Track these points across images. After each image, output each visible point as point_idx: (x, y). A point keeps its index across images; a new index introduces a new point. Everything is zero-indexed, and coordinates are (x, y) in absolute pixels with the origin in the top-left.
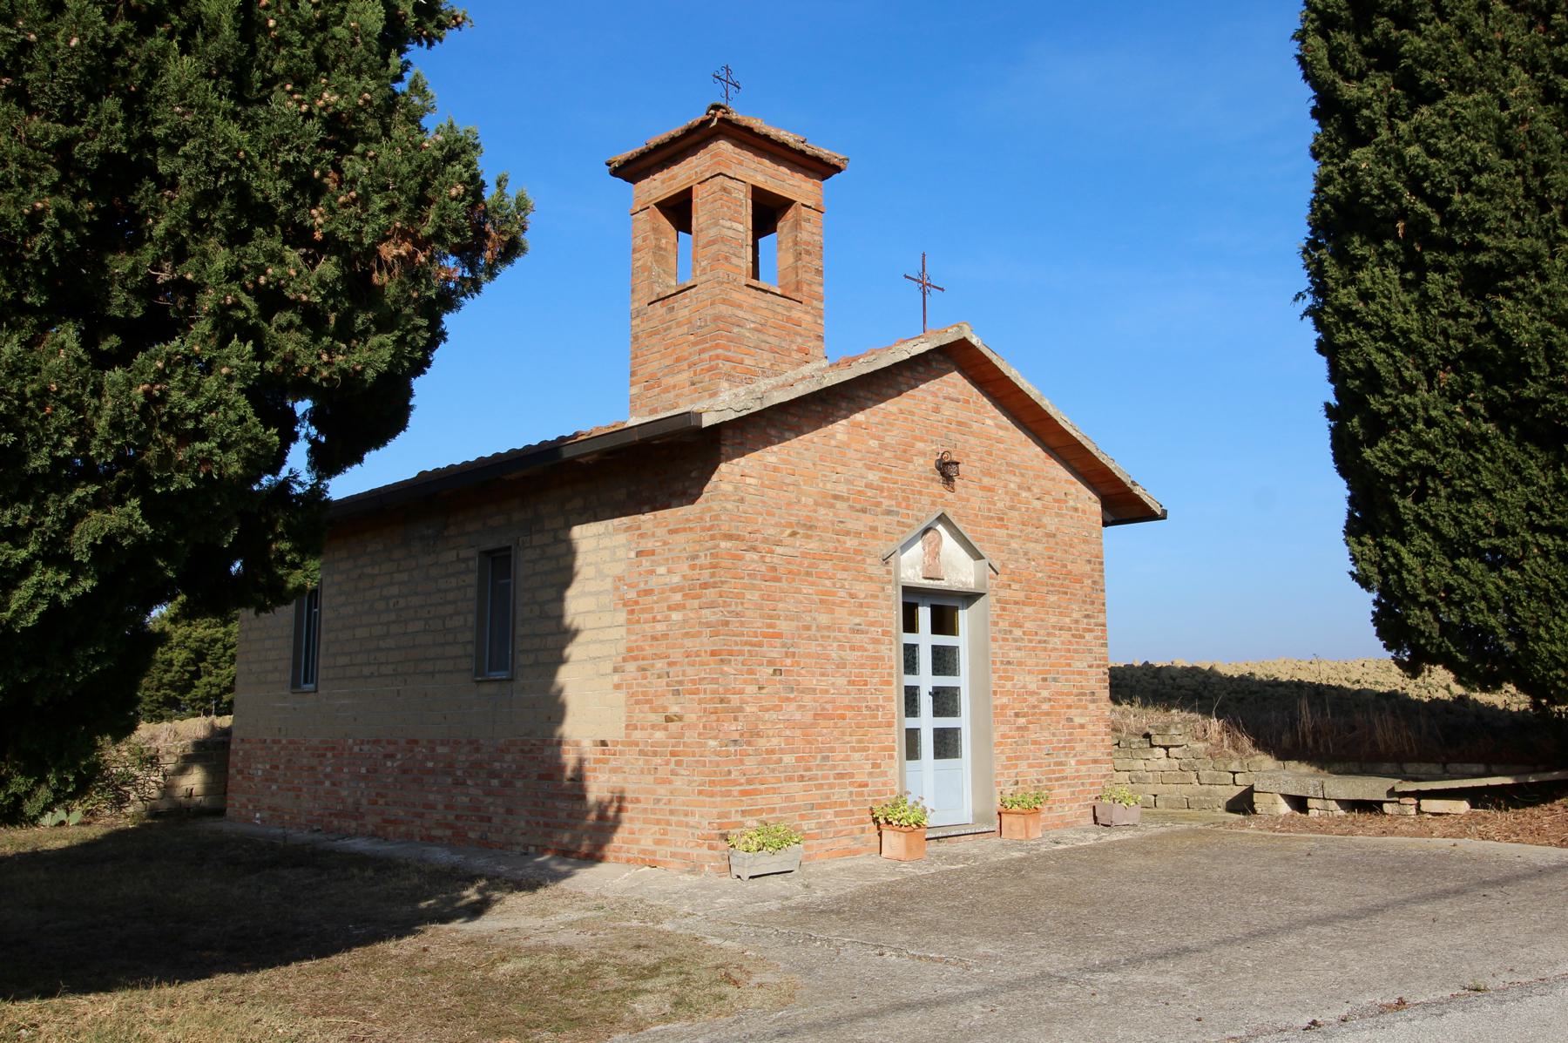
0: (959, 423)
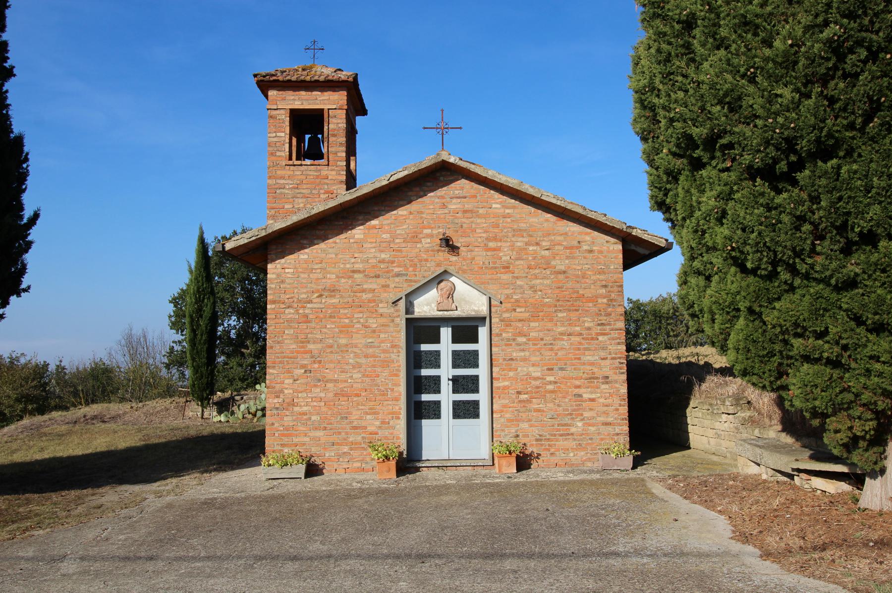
0: (465, 212)
